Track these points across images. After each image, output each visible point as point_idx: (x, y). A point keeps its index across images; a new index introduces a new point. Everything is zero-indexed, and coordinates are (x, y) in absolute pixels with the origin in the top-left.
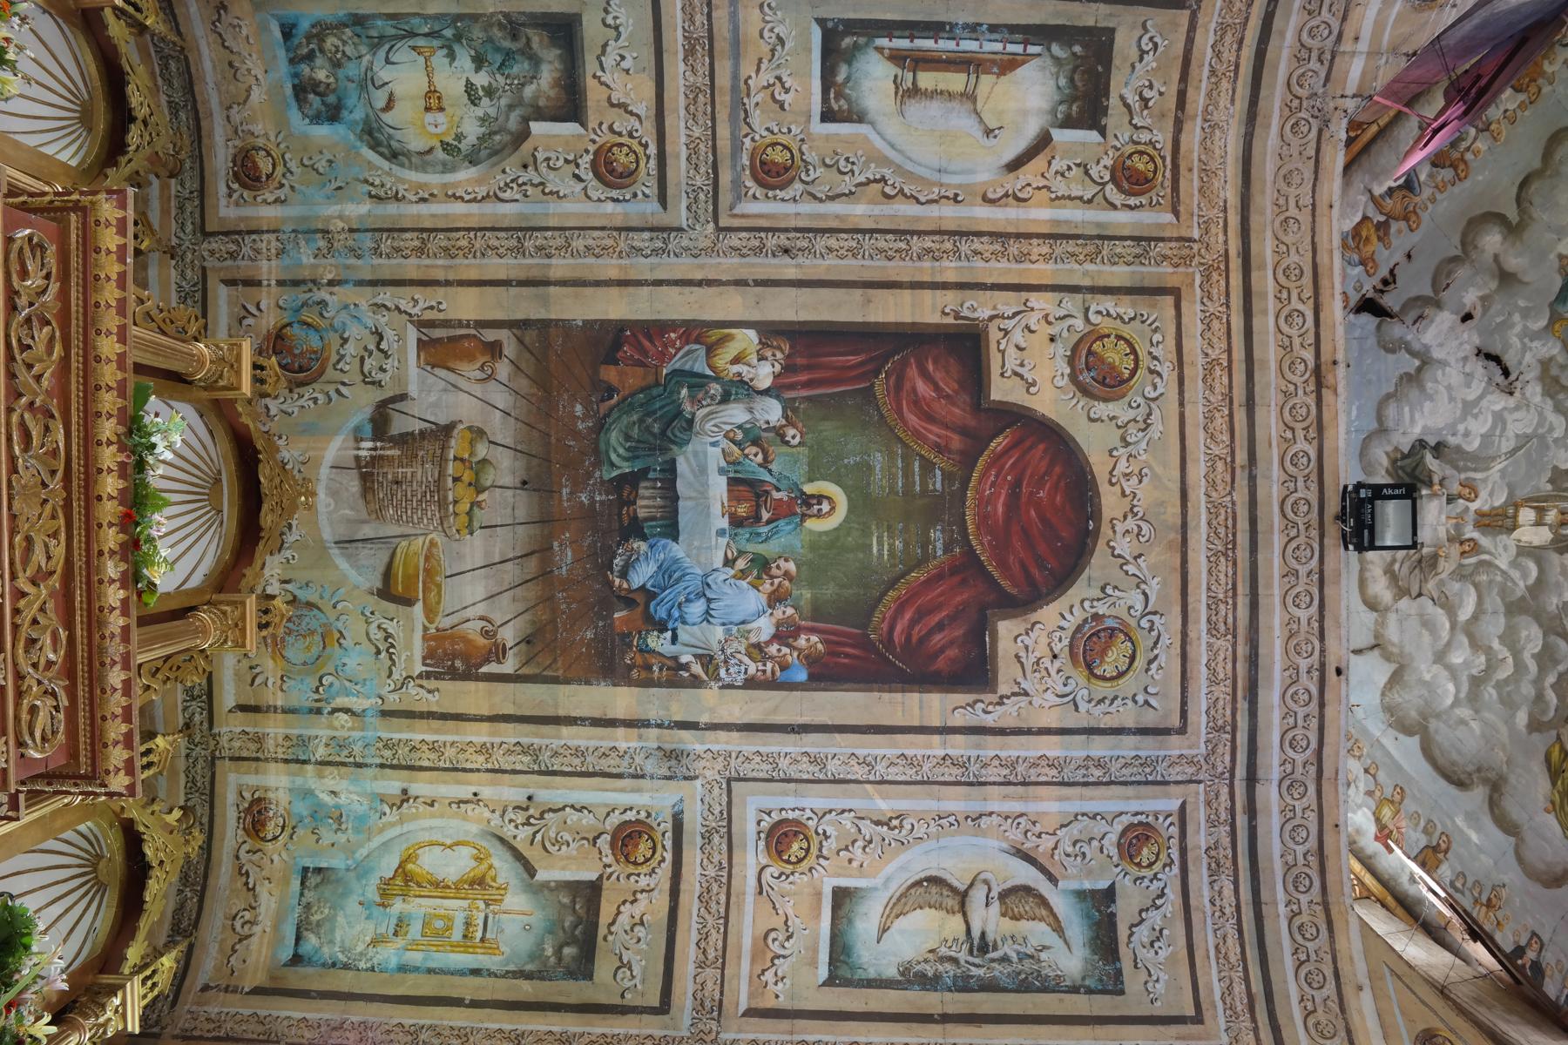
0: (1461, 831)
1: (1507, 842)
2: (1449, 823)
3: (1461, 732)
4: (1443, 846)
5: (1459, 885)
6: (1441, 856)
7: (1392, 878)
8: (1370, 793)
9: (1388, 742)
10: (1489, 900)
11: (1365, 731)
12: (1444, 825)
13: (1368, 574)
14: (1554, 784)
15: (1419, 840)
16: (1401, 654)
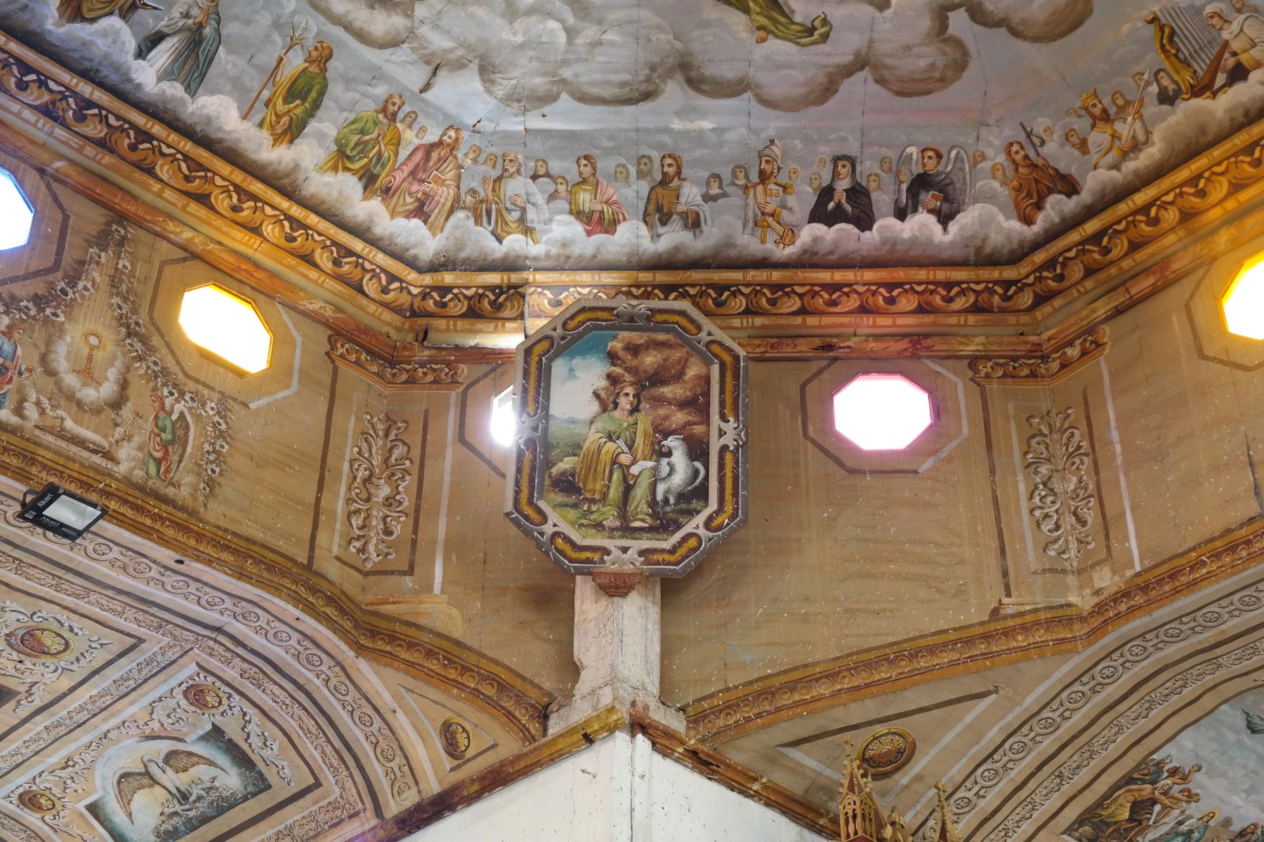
0: (688, 132)
1: (745, 101)
2: (666, 139)
3: (601, 57)
4: (671, 171)
5: (715, 191)
6: (676, 182)
7: (630, 255)
8: (553, 197)
9: (535, 122)
10: (762, 173)
11: (508, 136)
12: (659, 146)
13: (357, 24)
14: (746, 11)
15: (635, 192)
16: (470, 48)
